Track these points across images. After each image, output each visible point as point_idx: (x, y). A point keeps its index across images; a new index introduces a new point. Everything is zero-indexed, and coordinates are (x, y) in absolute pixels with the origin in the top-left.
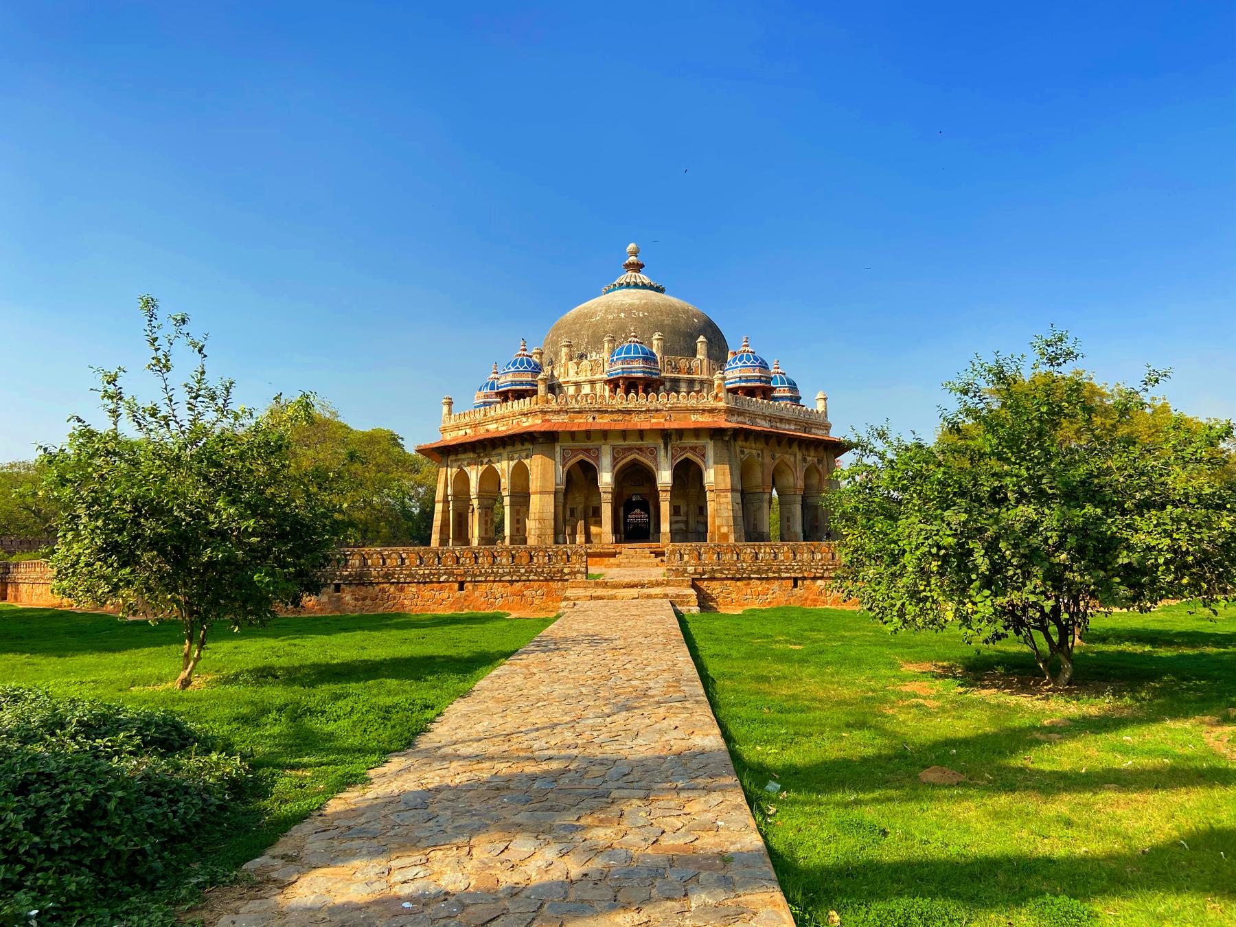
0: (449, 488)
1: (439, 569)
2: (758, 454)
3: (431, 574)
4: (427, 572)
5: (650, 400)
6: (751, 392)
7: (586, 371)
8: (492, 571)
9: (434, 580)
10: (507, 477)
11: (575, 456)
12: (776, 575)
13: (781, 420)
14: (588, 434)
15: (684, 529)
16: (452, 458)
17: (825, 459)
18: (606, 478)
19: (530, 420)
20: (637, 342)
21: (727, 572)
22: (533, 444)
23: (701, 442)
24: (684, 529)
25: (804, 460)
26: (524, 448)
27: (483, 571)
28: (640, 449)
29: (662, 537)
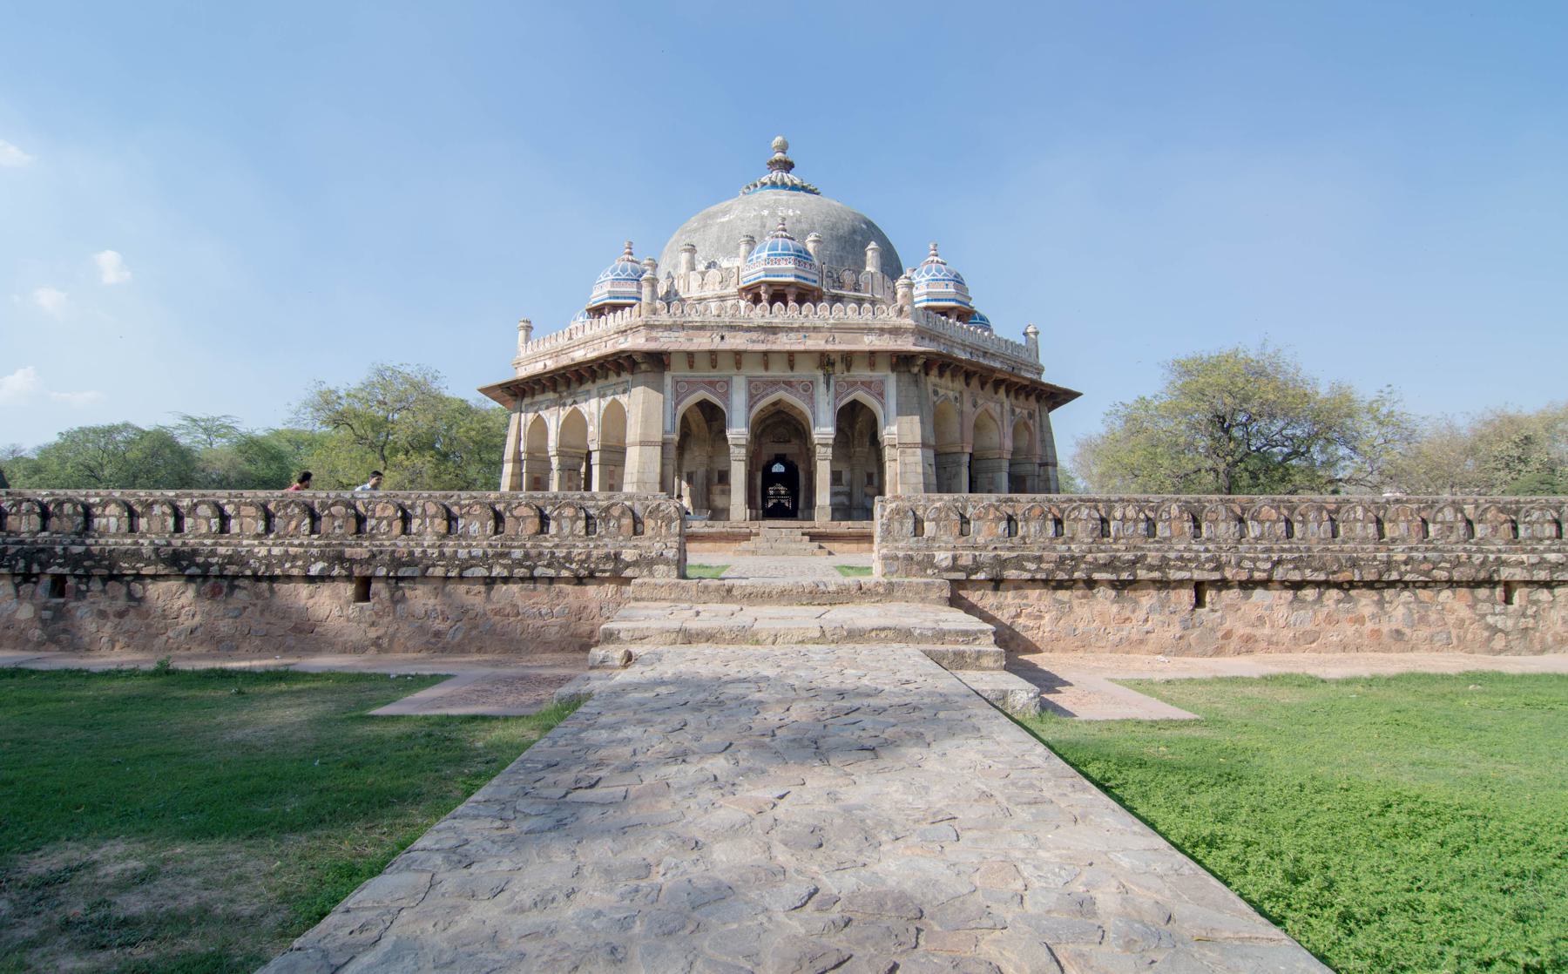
0: (522, 442)
4: (276, 551)
5: (804, 313)
9: (295, 572)
10: (596, 424)
14: (713, 356)
15: (847, 503)
16: (527, 401)
17: (1037, 414)
19: (629, 339)
21: (1032, 566)
22: (632, 373)
23: (877, 375)
24: (847, 503)
25: (1013, 411)
26: (621, 379)
28: (789, 384)
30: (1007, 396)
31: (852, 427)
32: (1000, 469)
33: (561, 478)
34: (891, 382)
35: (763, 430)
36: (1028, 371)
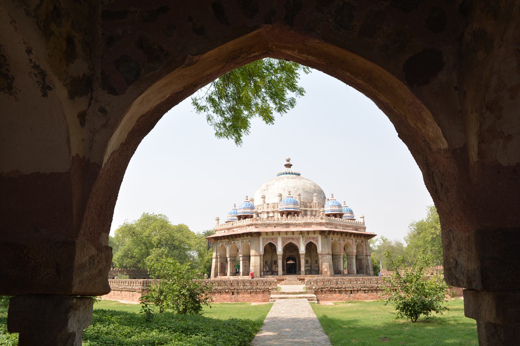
0: (218, 253)
2: (338, 240)
4: (221, 288)
5: (296, 219)
6: (335, 215)
11: (267, 242)
12: (344, 289)
13: (347, 226)
14: (273, 233)
17: (364, 241)
18: (280, 250)
21: (327, 288)
22: (251, 237)
23: (316, 236)
25: (356, 241)
26: (248, 238)
28: (293, 239)
29: (301, 273)
30: (354, 237)
31: (311, 248)
32: (353, 258)
33: (230, 263)
35: (286, 249)
36: (361, 229)
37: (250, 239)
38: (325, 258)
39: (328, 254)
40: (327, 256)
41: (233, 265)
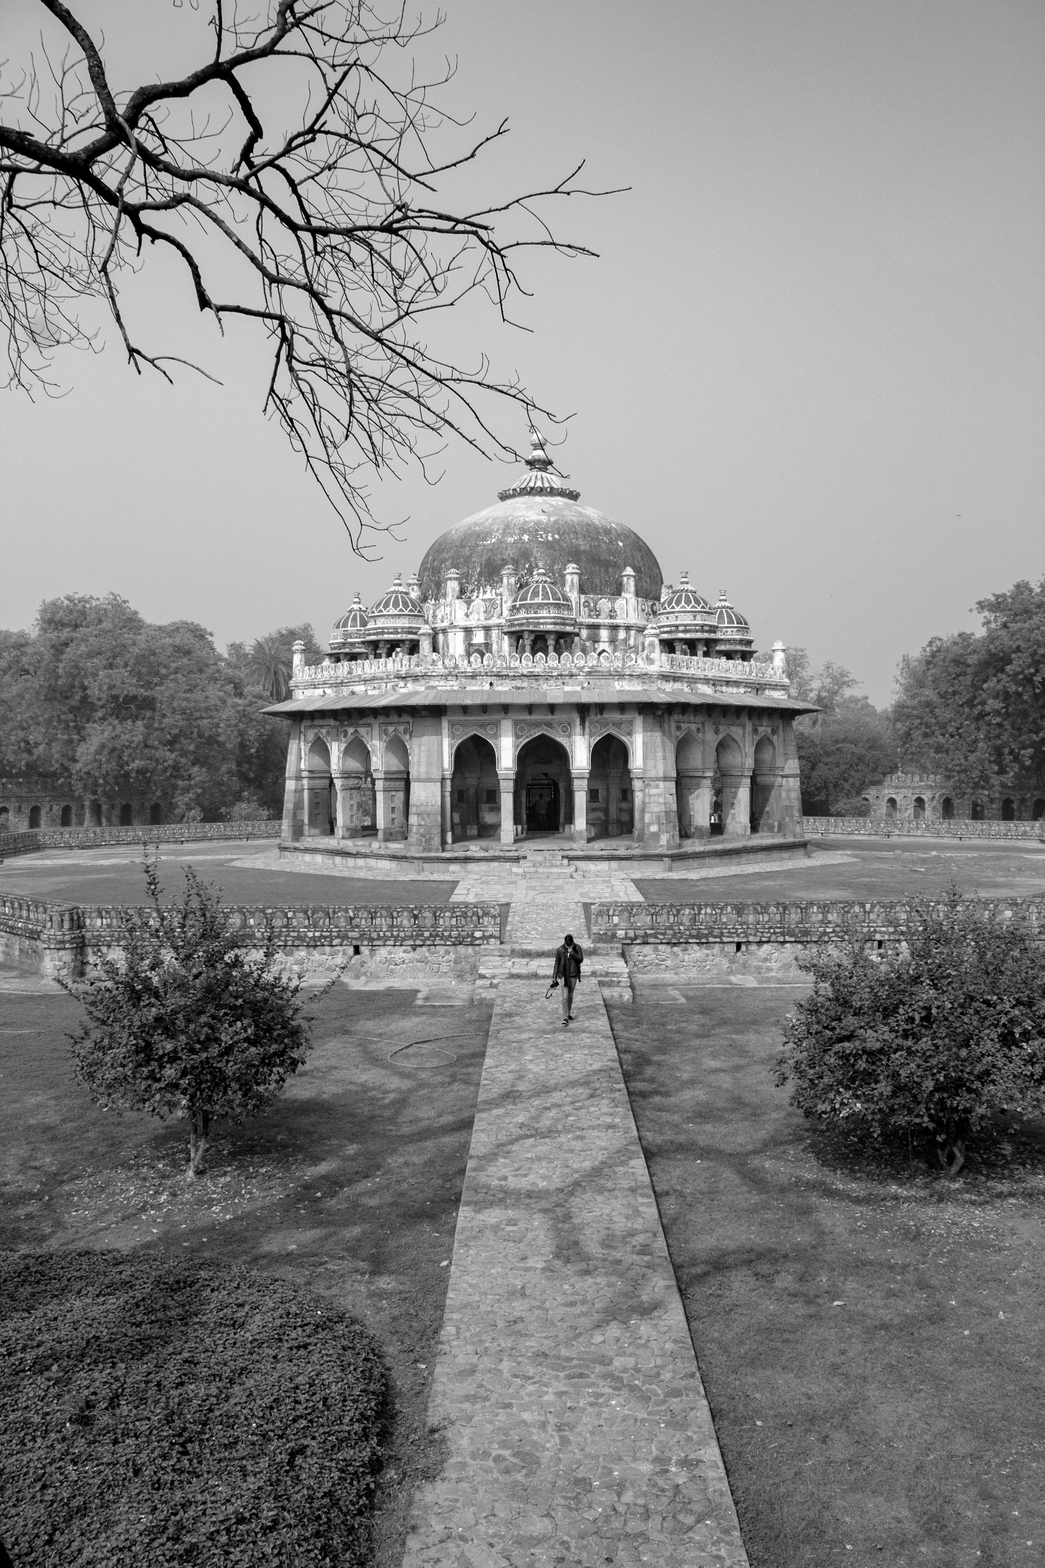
1: (331, 931)
3: (322, 936)
4: (317, 934)
5: (563, 662)
6: (692, 646)
7: (479, 613)
8: (392, 934)
12: (718, 940)
13: (728, 683)
15: (603, 818)
17: (781, 728)
19: (409, 685)
20: (546, 582)
23: (626, 717)
26: (402, 720)
27: (381, 934)
28: (549, 725)
30: (750, 718)
34: (639, 722)
37: (408, 723)
38: (653, 791)
39: (666, 779)
40: (661, 784)
41: (352, 802)
